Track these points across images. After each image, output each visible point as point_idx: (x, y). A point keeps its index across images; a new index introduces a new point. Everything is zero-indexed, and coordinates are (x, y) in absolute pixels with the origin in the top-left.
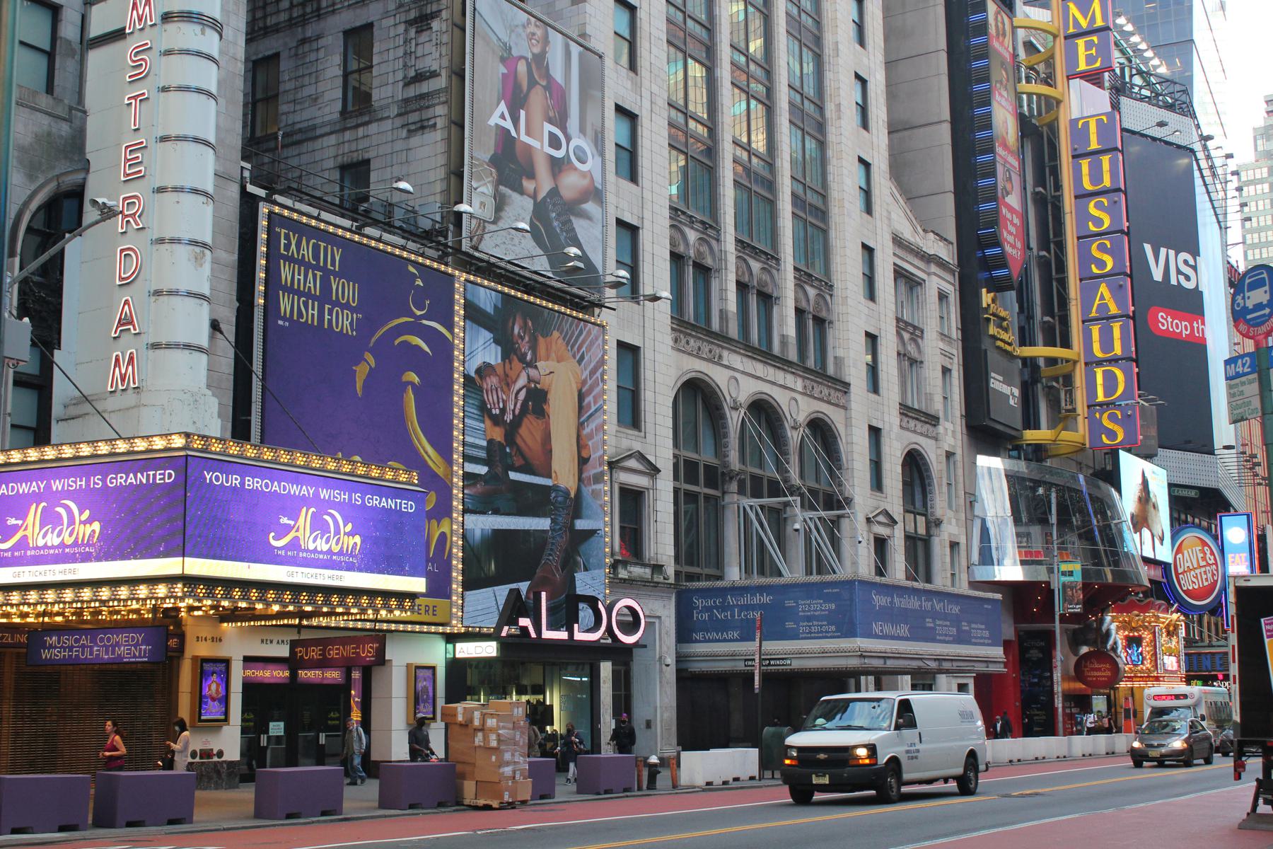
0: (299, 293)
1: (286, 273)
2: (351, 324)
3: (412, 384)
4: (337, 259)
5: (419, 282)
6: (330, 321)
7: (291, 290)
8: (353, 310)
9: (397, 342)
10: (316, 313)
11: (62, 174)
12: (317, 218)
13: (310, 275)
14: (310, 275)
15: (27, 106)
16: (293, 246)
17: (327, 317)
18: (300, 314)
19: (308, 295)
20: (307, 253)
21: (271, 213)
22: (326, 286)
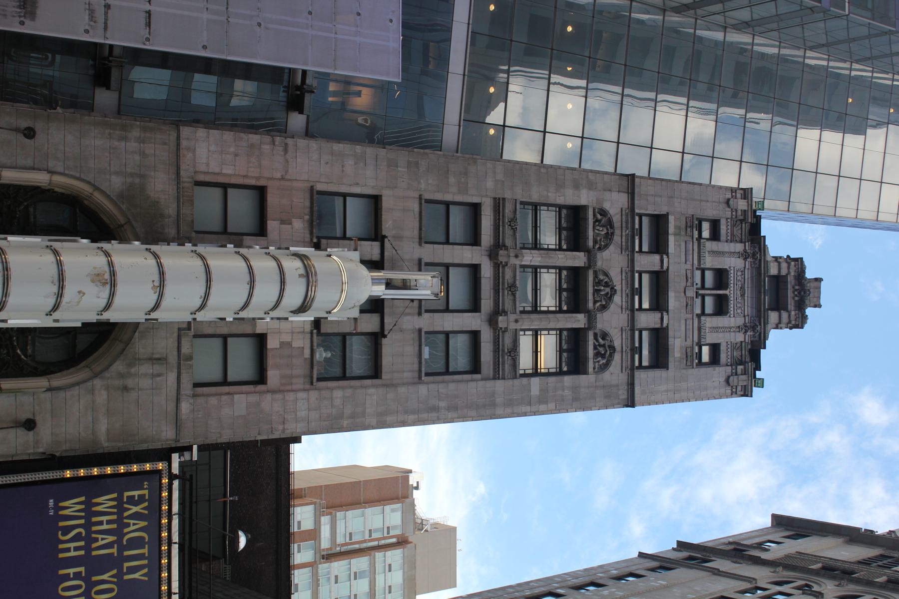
0: (88, 526)
1: (105, 502)
4: (136, 576)
6: (67, 577)
7: (89, 512)
10: (73, 554)
11: (133, 227)
13: (111, 539)
14: (111, 539)
15: (178, 193)
16: (135, 509)
17: (71, 571)
18: (67, 530)
19: (89, 540)
20: (134, 529)
21: (159, 472)
22: (104, 564)
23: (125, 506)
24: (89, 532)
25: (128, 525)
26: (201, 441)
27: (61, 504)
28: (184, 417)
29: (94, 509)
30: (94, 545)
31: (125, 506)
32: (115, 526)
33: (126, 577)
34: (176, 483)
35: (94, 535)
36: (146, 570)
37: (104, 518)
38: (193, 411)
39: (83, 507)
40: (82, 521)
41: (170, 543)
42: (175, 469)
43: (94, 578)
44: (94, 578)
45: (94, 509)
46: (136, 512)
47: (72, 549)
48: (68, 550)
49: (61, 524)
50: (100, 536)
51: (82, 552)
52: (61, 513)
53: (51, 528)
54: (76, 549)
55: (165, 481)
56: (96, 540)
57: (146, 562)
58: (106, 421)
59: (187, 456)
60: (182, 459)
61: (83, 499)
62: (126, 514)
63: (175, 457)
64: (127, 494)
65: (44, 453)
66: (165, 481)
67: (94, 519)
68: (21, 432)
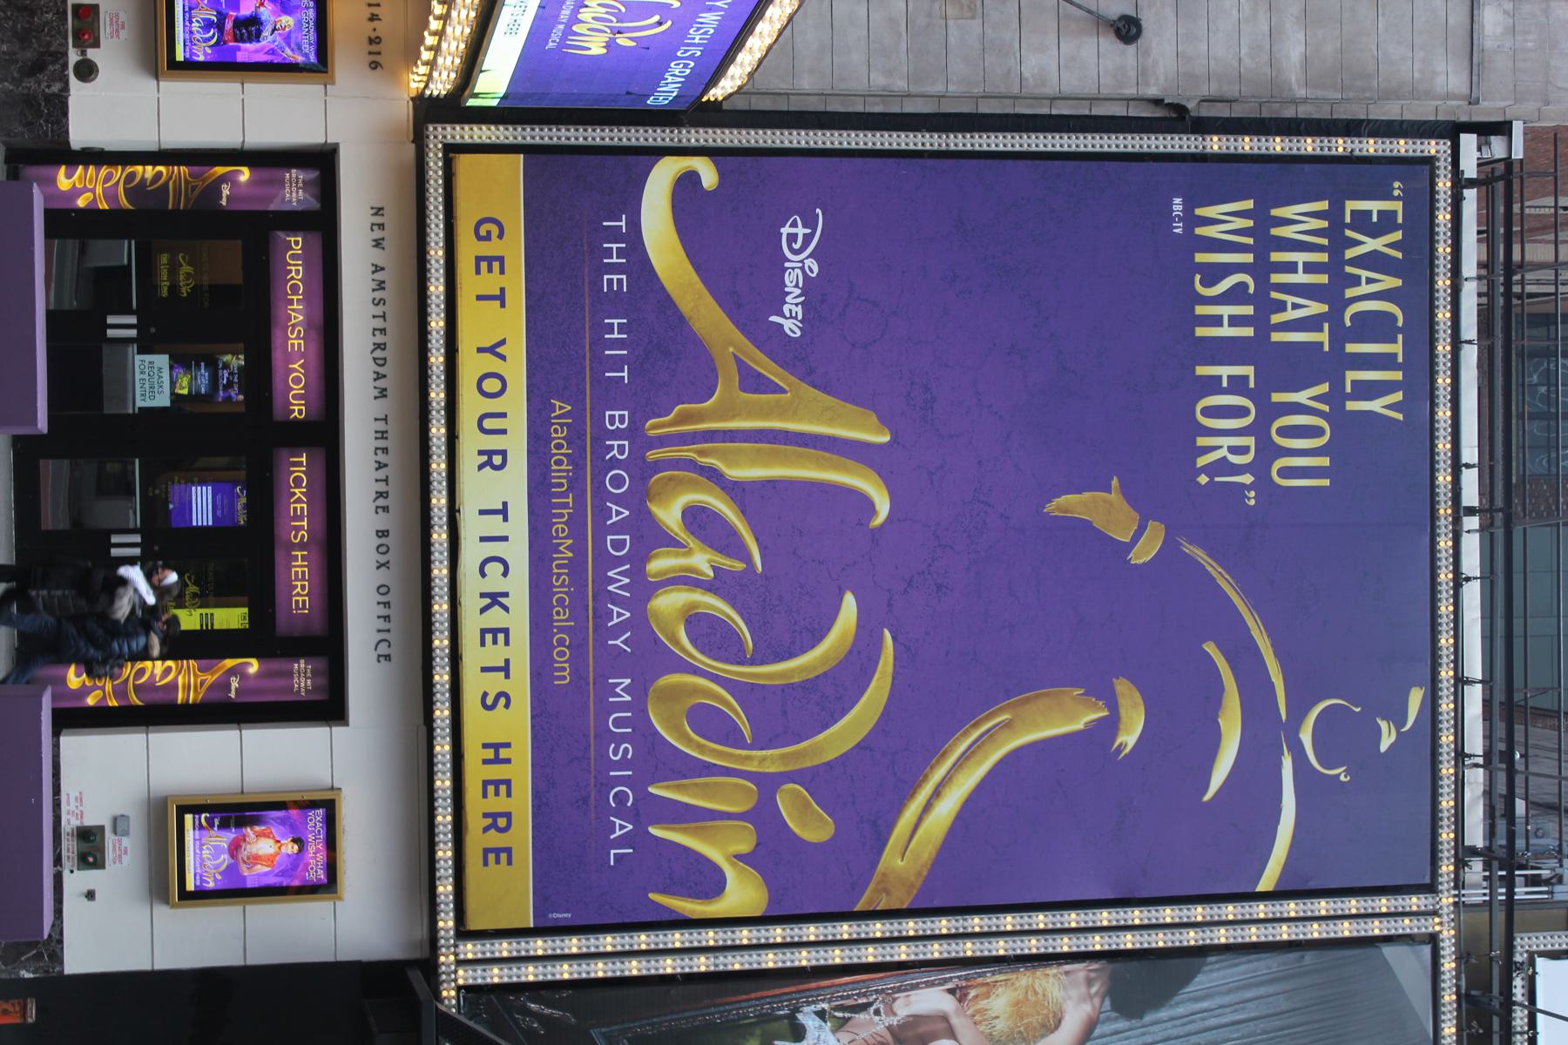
0: (1261, 269)
1: (1300, 219)
2: (1222, 466)
3: (1111, 725)
4: (1376, 406)
5: (1386, 743)
6: (1213, 385)
7: (1264, 240)
8: (1260, 467)
9: (1210, 648)
10: (1226, 331)
12: (1457, 343)
13: (1316, 308)
14: (1316, 308)
16: (1371, 244)
17: (1225, 371)
18: (1214, 274)
19: (1266, 306)
21: (1430, 161)
23: (1348, 233)
24: (1264, 285)
25: (1356, 281)
26: (1529, 107)
27: (1199, 212)
28: (1489, 44)
29: (1275, 232)
30: (1276, 319)
31: (1348, 233)
32: (1323, 279)
33: (1351, 406)
34: (1470, 195)
35: (1274, 295)
36: (1398, 397)
37: (1300, 257)
38: (1513, 31)
39: (1250, 223)
40: (1248, 258)
41: (1457, 467)
42: (1469, 168)
43: (1277, 397)
44: (1277, 397)
45: (1275, 232)
46: (1375, 251)
47: (1225, 321)
48: (1216, 321)
49: (1201, 258)
50: (1290, 299)
51: (1248, 332)
52: (1199, 231)
53: (1177, 264)
54: (1235, 321)
55: (1444, 185)
56: (1282, 306)
57: (1397, 376)
58: (1301, 36)
59: (1497, 148)
60: (1486, 155)
61: (1248, 204)
62: (1350, 253)
63: (1468, 141)
64: (1351, 205)
65: (1157, 102)
66: (1444, 185)
67: (1276, 257)
68: (1109, 43)
